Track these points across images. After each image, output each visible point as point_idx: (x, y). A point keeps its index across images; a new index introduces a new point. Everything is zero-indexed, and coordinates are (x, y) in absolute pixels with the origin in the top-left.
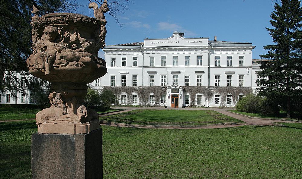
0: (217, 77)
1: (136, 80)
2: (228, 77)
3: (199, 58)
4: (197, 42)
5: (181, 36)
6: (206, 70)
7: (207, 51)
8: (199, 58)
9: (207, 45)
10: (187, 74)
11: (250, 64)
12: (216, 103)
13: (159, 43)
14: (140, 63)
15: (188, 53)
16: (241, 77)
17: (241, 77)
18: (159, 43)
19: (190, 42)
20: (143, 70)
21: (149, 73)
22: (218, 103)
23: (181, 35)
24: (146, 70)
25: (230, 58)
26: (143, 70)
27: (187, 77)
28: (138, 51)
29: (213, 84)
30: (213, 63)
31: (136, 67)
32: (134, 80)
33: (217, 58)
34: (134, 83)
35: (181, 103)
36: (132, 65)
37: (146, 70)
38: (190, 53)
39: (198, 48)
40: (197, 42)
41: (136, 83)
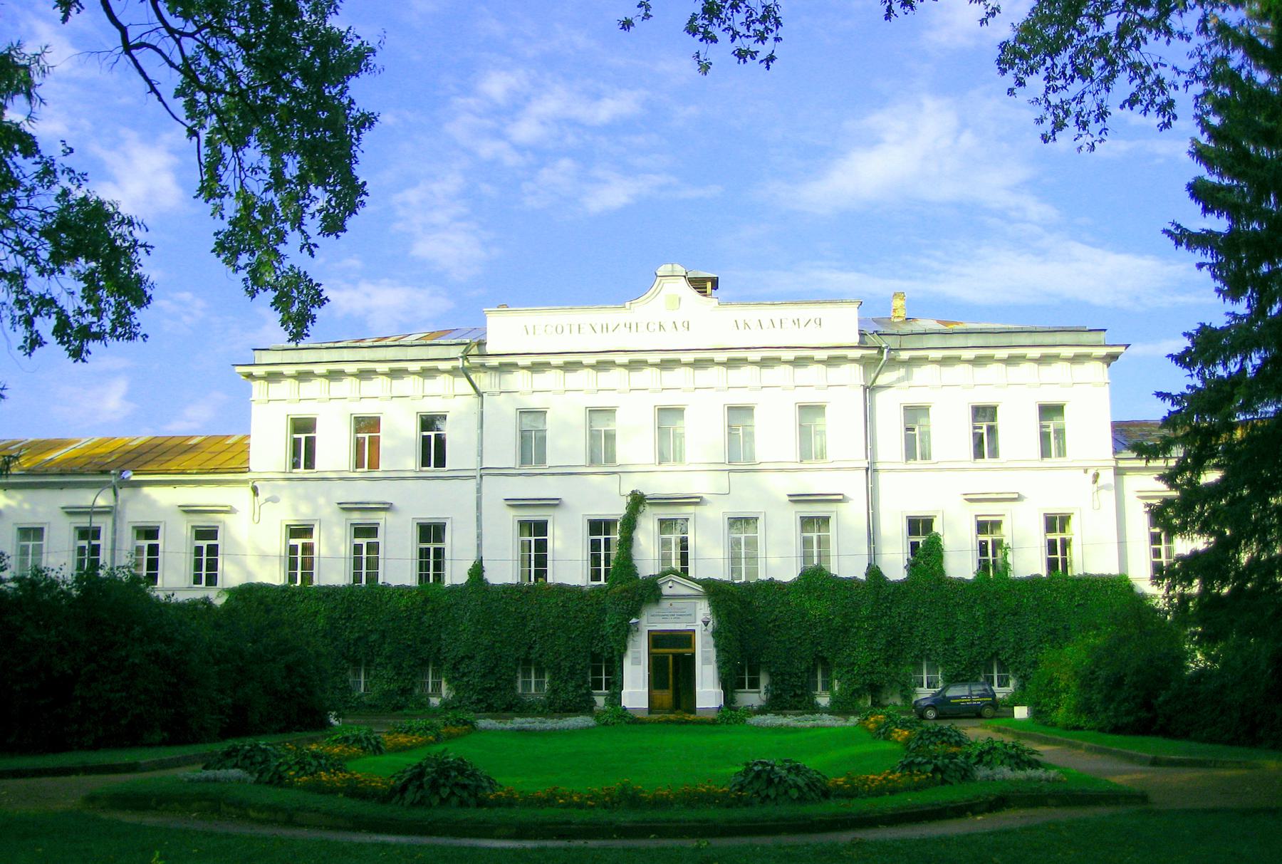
1: (439, 553)
2: (982, 527)
4: (796, 322)
5: (703, 292)
6: (854, 486)
9: (855, 340)
13: (575, 329)
19: (754, 324)
20: (479, 490)
23: (699, 284)
25: (984, 413)
26: (479, 490)
28: (454, 372)
29: (895, 566)
31: (440, 472)
32: (424, 553)
33: (914, 414)
34: (198, 565)
36: (411, 462)
40: (796, 322)
41: (439, 566)
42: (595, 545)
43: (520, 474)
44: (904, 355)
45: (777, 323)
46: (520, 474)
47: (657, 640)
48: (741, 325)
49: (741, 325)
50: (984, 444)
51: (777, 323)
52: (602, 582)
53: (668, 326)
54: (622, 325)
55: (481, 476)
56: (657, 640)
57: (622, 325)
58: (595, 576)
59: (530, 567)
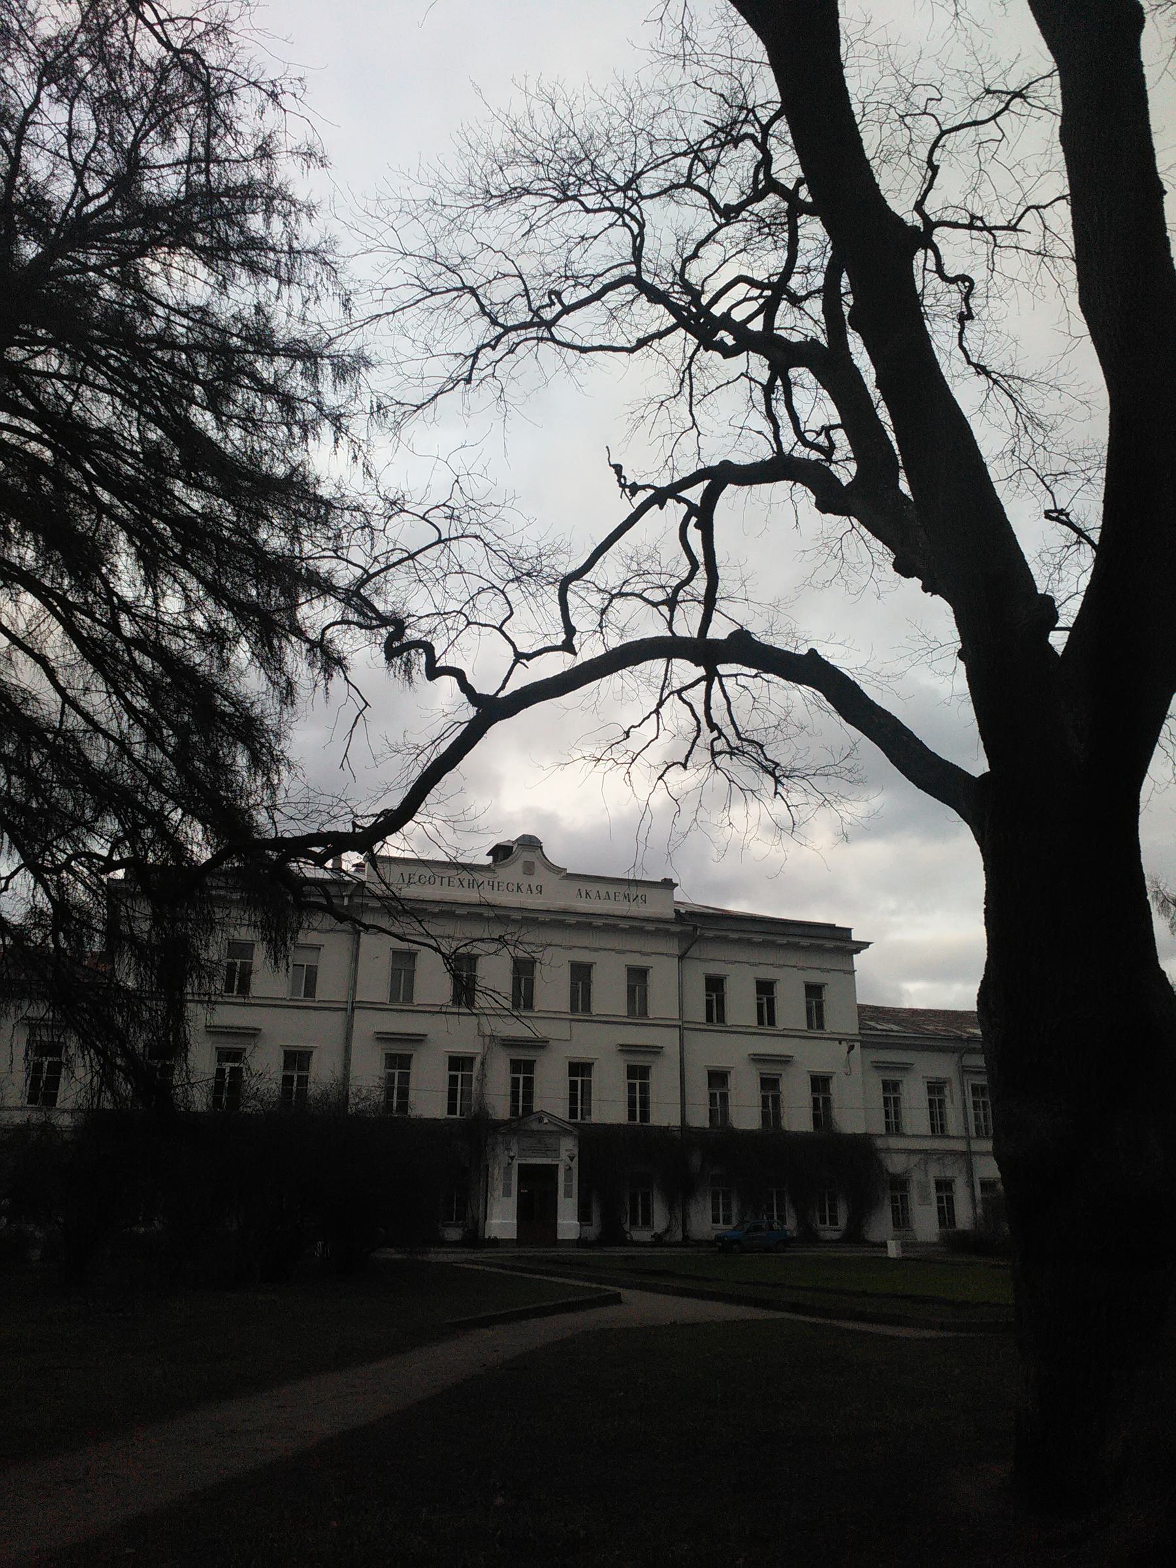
0: (718, 1078)
3: (638, 976)
6: (668, 1039)
7: (673, 947)
8: (638, 976)
9: (672, 915)
10: (580, 1054)
11: (852, 1027)
12: (715, 1220)
13: (446, 881)
14: (330, 987)
15: (581, 948)
16: (820, 1083)
17: (820, 1083)
18: (446, 881)
19: (593, 894)
21: (383, 1038)
22: (727, 1221)
24: (367, 1024)
25: (765, 988)
27: (580, 1069)
30: (697, 1010)
33: (715, 985)
35: (568, 1224)
37: (367, 1024)
38: (595, 950)
39: (638, 927)
40: (627, 897)
42: (453, 1080)
43: (391, 1010)
44: (710, 934)
45: (612, 896)
46: (391, 1010)
47: (526, 1172)
48: (584, 894)
49: (584, 894)
50: (766, 1012)
51: (612, 896)
52: (458, 1116)
53: (524, 888)
54: (486, 883)
55: (353, 1010)
56: (526, 1172)
57: (486, 883)
58: (452, 1109)
59: (582, 1109)
